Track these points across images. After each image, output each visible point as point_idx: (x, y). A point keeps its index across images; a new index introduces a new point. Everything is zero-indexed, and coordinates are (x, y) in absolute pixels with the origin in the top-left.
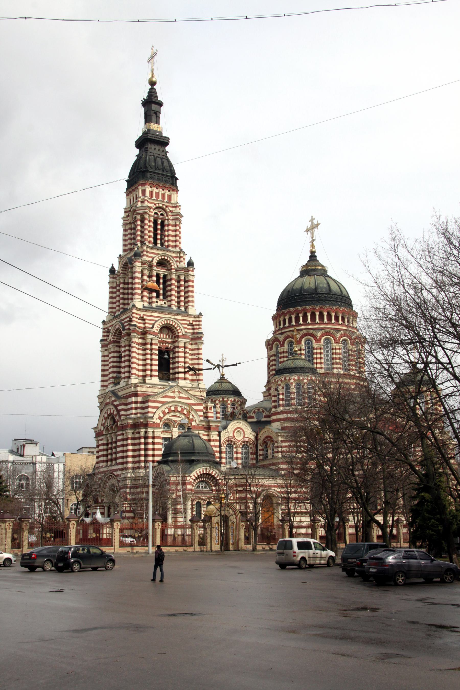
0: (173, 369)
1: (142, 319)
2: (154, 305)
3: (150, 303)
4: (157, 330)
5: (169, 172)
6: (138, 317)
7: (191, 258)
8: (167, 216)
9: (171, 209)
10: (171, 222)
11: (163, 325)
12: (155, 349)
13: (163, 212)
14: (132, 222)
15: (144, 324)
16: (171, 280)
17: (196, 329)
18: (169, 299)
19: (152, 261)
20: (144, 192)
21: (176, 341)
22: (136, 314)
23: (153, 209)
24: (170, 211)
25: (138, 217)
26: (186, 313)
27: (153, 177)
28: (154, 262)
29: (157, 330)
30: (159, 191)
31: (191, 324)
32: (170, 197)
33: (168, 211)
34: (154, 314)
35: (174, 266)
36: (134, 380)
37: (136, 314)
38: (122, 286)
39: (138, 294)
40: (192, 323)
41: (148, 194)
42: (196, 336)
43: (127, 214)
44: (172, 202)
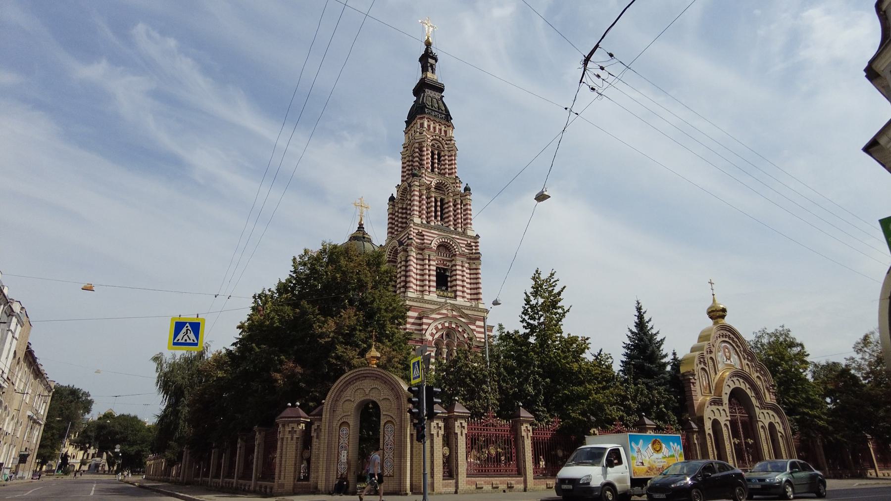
0: (451, 287)
1: (420, 234)
2: (432, 224)
3: (428, 222)
4: (434, 246)
6: (417, 231)
7: (467, 184)
8: (443, 147)
9: (448, 142)
10: (447, 153)
11: (440, 242)
12: (433, 265)
13: (441, 145)
14: (410, 155)
15: (423, 240)
16: (447, 203)
18: (446, 220)
19: (431, 183)
20: (422, 125)
21: (453, 260)
25: (417, 145)
26: (464, 233)
27: (430, 113)
28: (432, 185)
29: (434, 246)
31: (469, 245)
32: (445, 132)
34: (432, 231)
35: (451, 189)
36: (411, 294)
38: (400, 211)
41: (426, 125)
42: (473, 256)
43: (406, 149)
44: (448, 136)
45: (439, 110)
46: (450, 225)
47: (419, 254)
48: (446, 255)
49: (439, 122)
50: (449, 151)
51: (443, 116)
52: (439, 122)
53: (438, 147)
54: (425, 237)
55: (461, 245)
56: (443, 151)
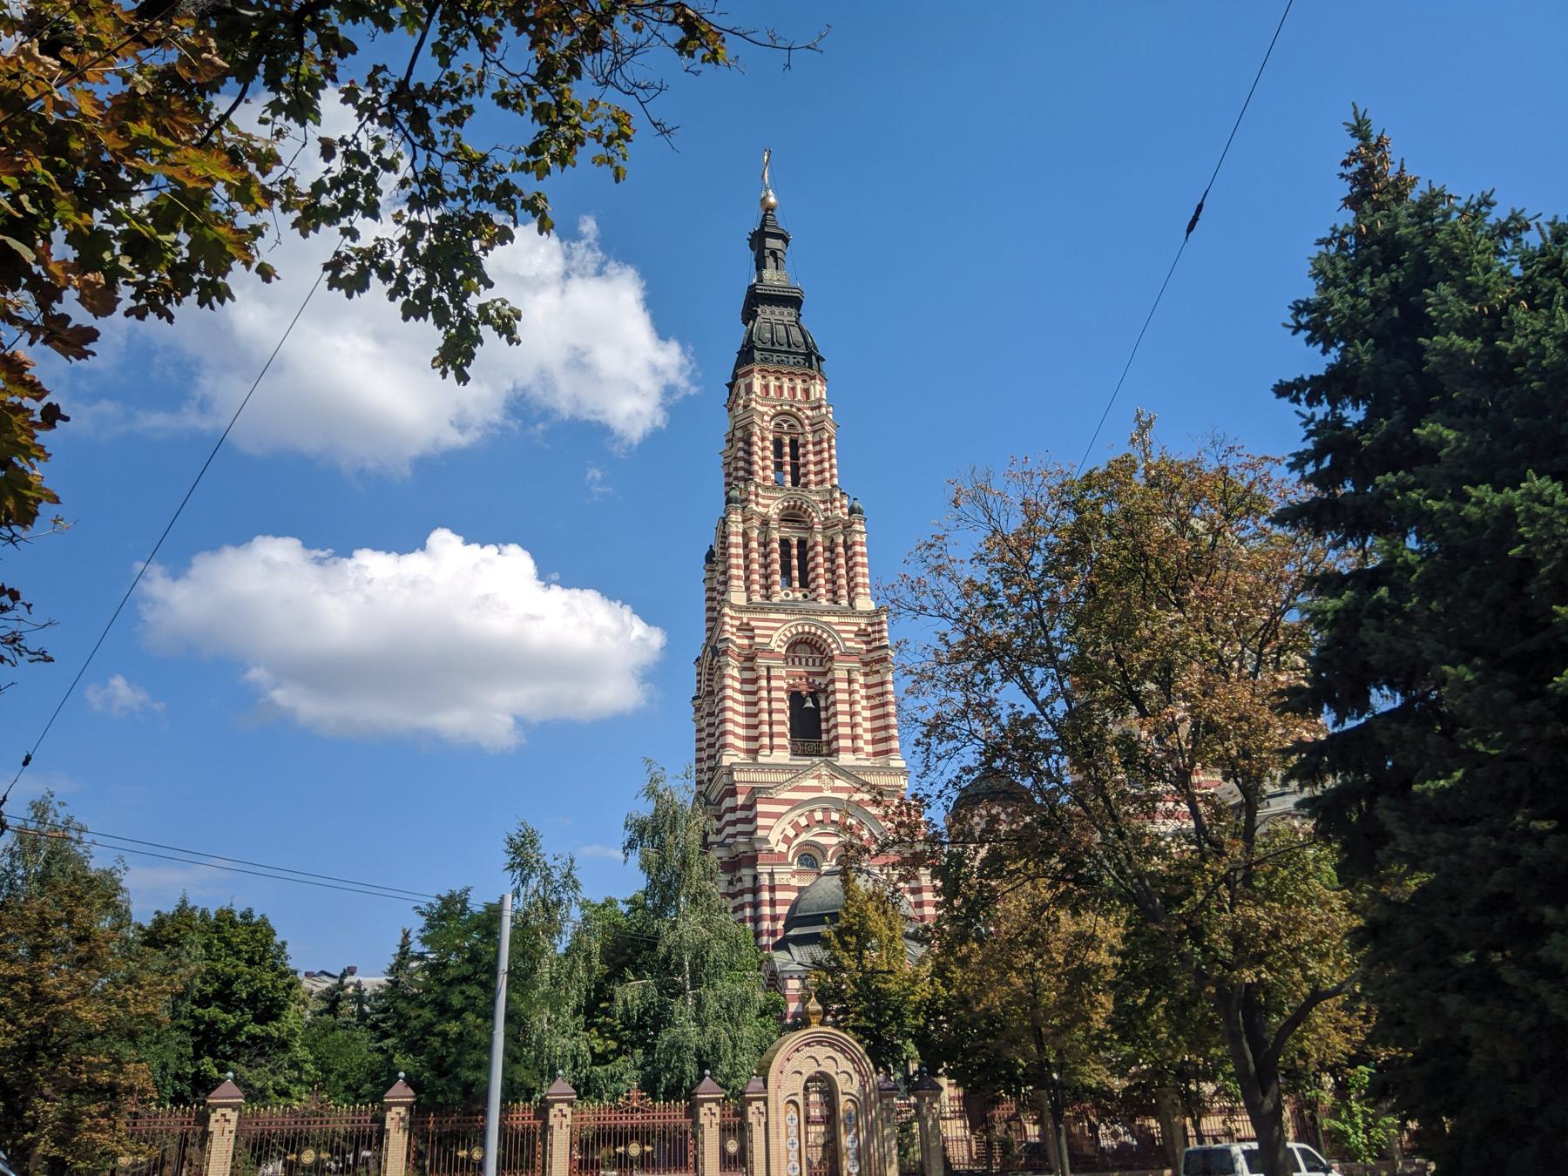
1: (746, 628)
2: (775, 599)
6: (737, 623)
9: (809, 413)
13: (793, 421)
15: (752, 638)
21: (830, 669)
22: (732, 618)
24: (808, 417)
32: (806, 392)
35: (817, 519)
37: (732, 618)
39: (738, 578)
40: (865, 630)
41: (757, 388)
42: (875, 655)
47: (745, 669)
48: (814, 661)
49: (789, 373)
50: (815, 432)
51: (800, 358)
52: (789, 373)
54: (757, 631)
55: (843, 635)
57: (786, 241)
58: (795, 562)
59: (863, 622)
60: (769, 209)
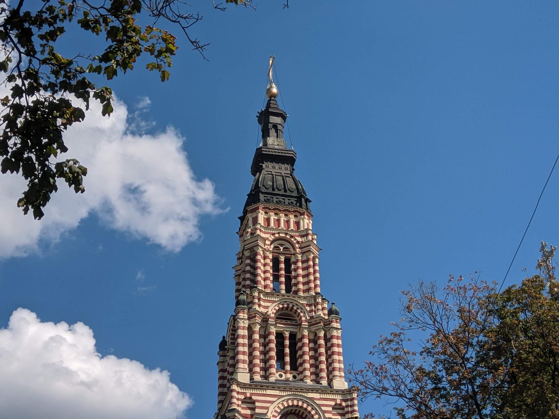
2: (272, 379)
5: (296, 192)
6: (242, 397)
9: (299, 239)
13: (288, 245)
15: (253, 409)
17: (348, 412)
22: (238, 393)
23: (269, 240)
24: (298, 242)
30: (280, 217)
32: (297, 224)
33: (295, 242)
34: (269, 392)
37: (238, 393)
39: (244, 362)
40: (340, 405)
45: (285, 191)
46: (305, 376)
49: (285, 210)
51: (293, 200)
52: (285, 210)
53: (286, 248)
54: (257, 404)
55: (324, 408)
56: (294, 254)
57: (284, 118)
58: (287, 350)
59: (339, 398)
60: (272, 96)
